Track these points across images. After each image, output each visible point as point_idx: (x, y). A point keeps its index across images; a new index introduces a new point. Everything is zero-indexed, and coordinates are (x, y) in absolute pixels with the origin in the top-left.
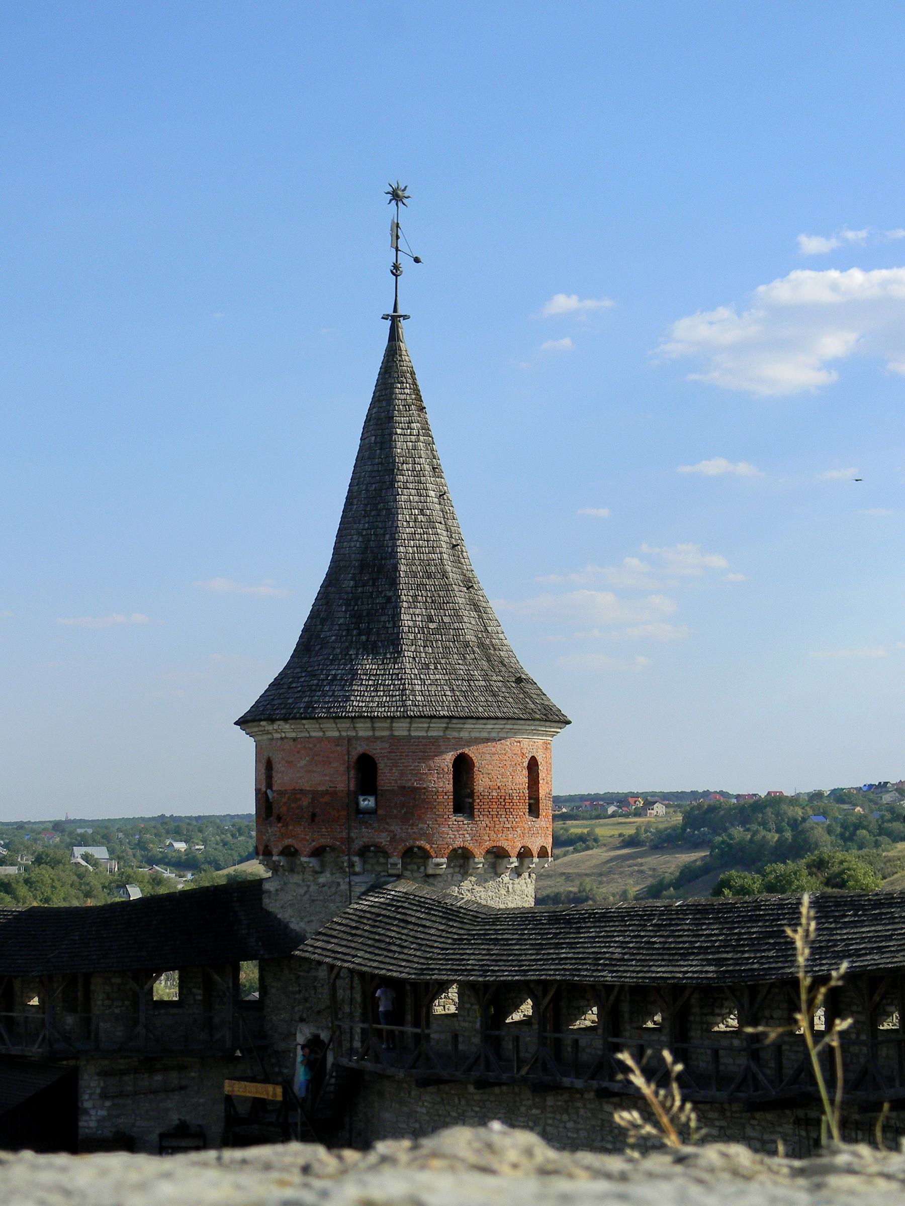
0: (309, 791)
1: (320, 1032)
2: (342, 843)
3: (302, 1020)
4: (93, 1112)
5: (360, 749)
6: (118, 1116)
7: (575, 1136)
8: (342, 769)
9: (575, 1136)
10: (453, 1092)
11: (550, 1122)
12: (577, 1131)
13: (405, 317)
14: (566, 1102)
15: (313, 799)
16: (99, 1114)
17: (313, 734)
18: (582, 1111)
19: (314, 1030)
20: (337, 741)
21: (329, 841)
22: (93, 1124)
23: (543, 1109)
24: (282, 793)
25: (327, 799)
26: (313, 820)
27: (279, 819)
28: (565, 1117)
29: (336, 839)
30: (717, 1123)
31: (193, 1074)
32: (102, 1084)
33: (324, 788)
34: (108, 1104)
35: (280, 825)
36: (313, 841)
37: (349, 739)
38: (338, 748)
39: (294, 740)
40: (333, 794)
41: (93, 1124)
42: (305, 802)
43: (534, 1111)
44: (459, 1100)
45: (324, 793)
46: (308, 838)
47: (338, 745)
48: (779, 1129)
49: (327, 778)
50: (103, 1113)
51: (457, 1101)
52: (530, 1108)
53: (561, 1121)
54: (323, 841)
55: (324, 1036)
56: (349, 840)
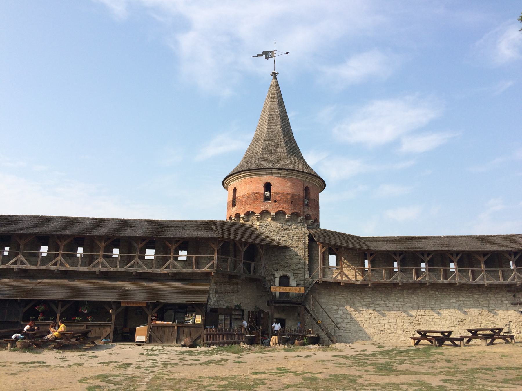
0: (291, 194)
1: (288, 273)
2: (301, 212)
3: (277, 270)
4: (212, 299)
5: (306, 185)
6: (219, 301)
7: (418, 301)
8: (302, 189)
9: (418, 301)
10: (358, 291)
11: (406, 298)
12: (418, 300)
13: (278, 74)
14: (413, 291)
15: (292, 197)
16: (214, 299)
17: (292, 177)
18: (420, 294)
19: (284, 273)
20: (300, 181)
21: (297, 211)
22: (212, 304)
23: (402, 294)
24: (277, 193)
25: (297, 197)
26: (292, 203)
27: (275, 201)
28: (413, 296)
29: (299, 211)
30: (477, 294)
31: (240, 287)
32: (216, 288)
33: (296, 194)
34: (217, 296)
35: (275, 203)
36: (292, 210)
37: (304, 181)
38: (300, 183)
39: (284, 177)
40: (299, 196)
41: (212, 304)
42: (289, 197)
43: (398, 295)
44: (361, 294)
45: (296, 195)
46: (290, 208)
47: (300, 182)
48: (500, 294)
49: (297, 191)
50: (215, 299)
51: (360, 293)
52: (396, 294)
53: (411, 297)
54: (295, 211)
55: (289, 275)
56: (304, 212)
